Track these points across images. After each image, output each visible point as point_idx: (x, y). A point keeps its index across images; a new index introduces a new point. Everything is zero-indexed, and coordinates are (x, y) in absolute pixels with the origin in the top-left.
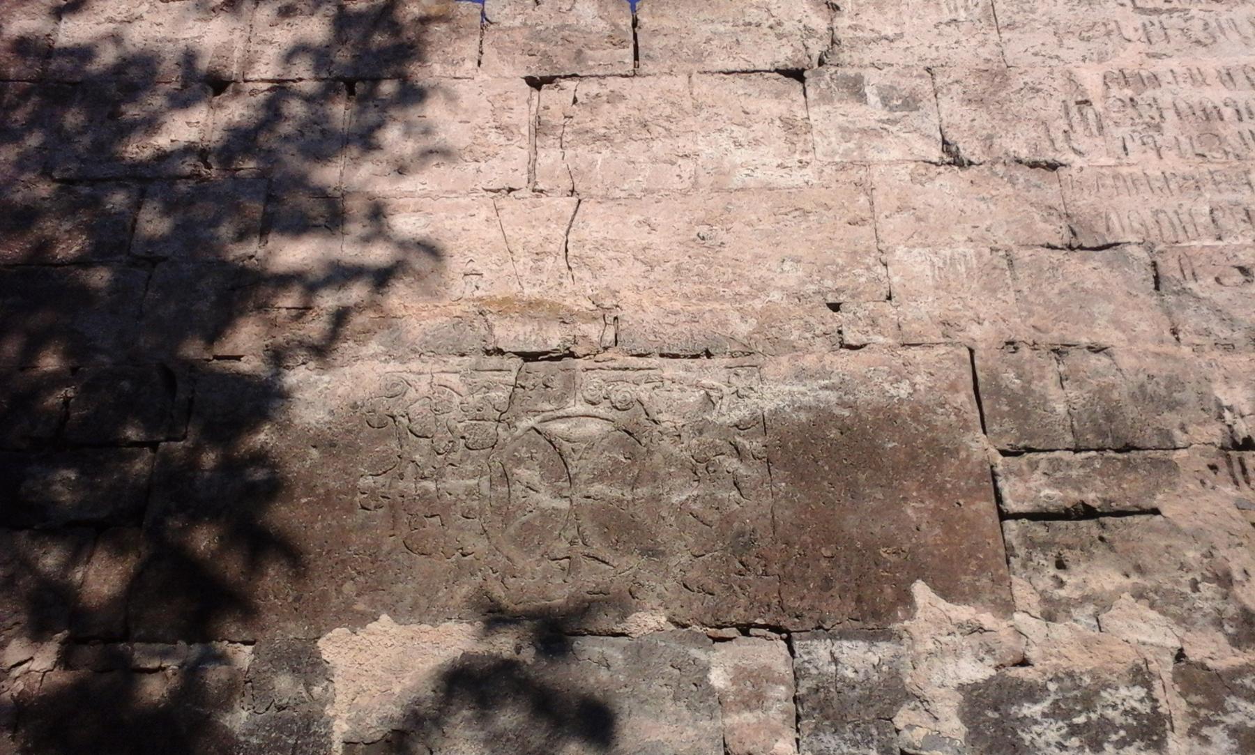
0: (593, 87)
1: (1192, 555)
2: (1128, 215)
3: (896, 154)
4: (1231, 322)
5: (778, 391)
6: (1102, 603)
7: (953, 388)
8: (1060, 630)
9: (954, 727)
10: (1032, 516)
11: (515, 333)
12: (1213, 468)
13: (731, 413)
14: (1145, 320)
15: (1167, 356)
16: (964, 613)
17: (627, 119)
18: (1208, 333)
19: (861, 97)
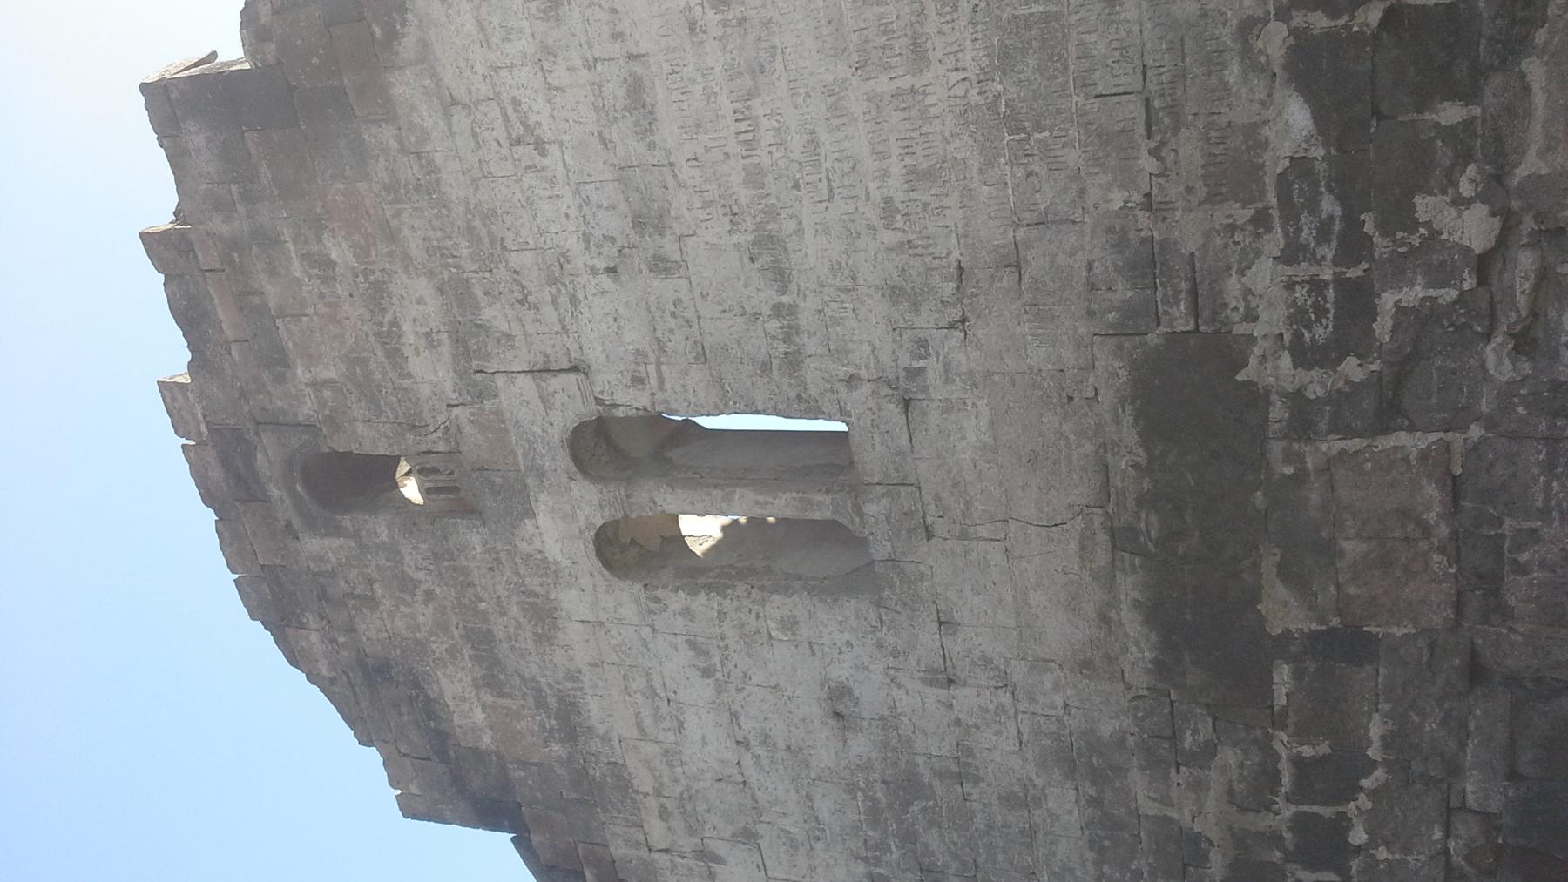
1: (1218, 241)
3: (962, 357)
5: (1130, 436)
6: (1247, 292)
7: (1120, 347)
8: (1264, 316)
9: (1315, 373)
10: (1197, 317)
11: (1102, 557)
12: (1164, 219)
13: (1142, 457)
15: (1093, 232)
16: (1253, 361)
17: (953, 494)
18: (1073, 201)
19: (921, 370)
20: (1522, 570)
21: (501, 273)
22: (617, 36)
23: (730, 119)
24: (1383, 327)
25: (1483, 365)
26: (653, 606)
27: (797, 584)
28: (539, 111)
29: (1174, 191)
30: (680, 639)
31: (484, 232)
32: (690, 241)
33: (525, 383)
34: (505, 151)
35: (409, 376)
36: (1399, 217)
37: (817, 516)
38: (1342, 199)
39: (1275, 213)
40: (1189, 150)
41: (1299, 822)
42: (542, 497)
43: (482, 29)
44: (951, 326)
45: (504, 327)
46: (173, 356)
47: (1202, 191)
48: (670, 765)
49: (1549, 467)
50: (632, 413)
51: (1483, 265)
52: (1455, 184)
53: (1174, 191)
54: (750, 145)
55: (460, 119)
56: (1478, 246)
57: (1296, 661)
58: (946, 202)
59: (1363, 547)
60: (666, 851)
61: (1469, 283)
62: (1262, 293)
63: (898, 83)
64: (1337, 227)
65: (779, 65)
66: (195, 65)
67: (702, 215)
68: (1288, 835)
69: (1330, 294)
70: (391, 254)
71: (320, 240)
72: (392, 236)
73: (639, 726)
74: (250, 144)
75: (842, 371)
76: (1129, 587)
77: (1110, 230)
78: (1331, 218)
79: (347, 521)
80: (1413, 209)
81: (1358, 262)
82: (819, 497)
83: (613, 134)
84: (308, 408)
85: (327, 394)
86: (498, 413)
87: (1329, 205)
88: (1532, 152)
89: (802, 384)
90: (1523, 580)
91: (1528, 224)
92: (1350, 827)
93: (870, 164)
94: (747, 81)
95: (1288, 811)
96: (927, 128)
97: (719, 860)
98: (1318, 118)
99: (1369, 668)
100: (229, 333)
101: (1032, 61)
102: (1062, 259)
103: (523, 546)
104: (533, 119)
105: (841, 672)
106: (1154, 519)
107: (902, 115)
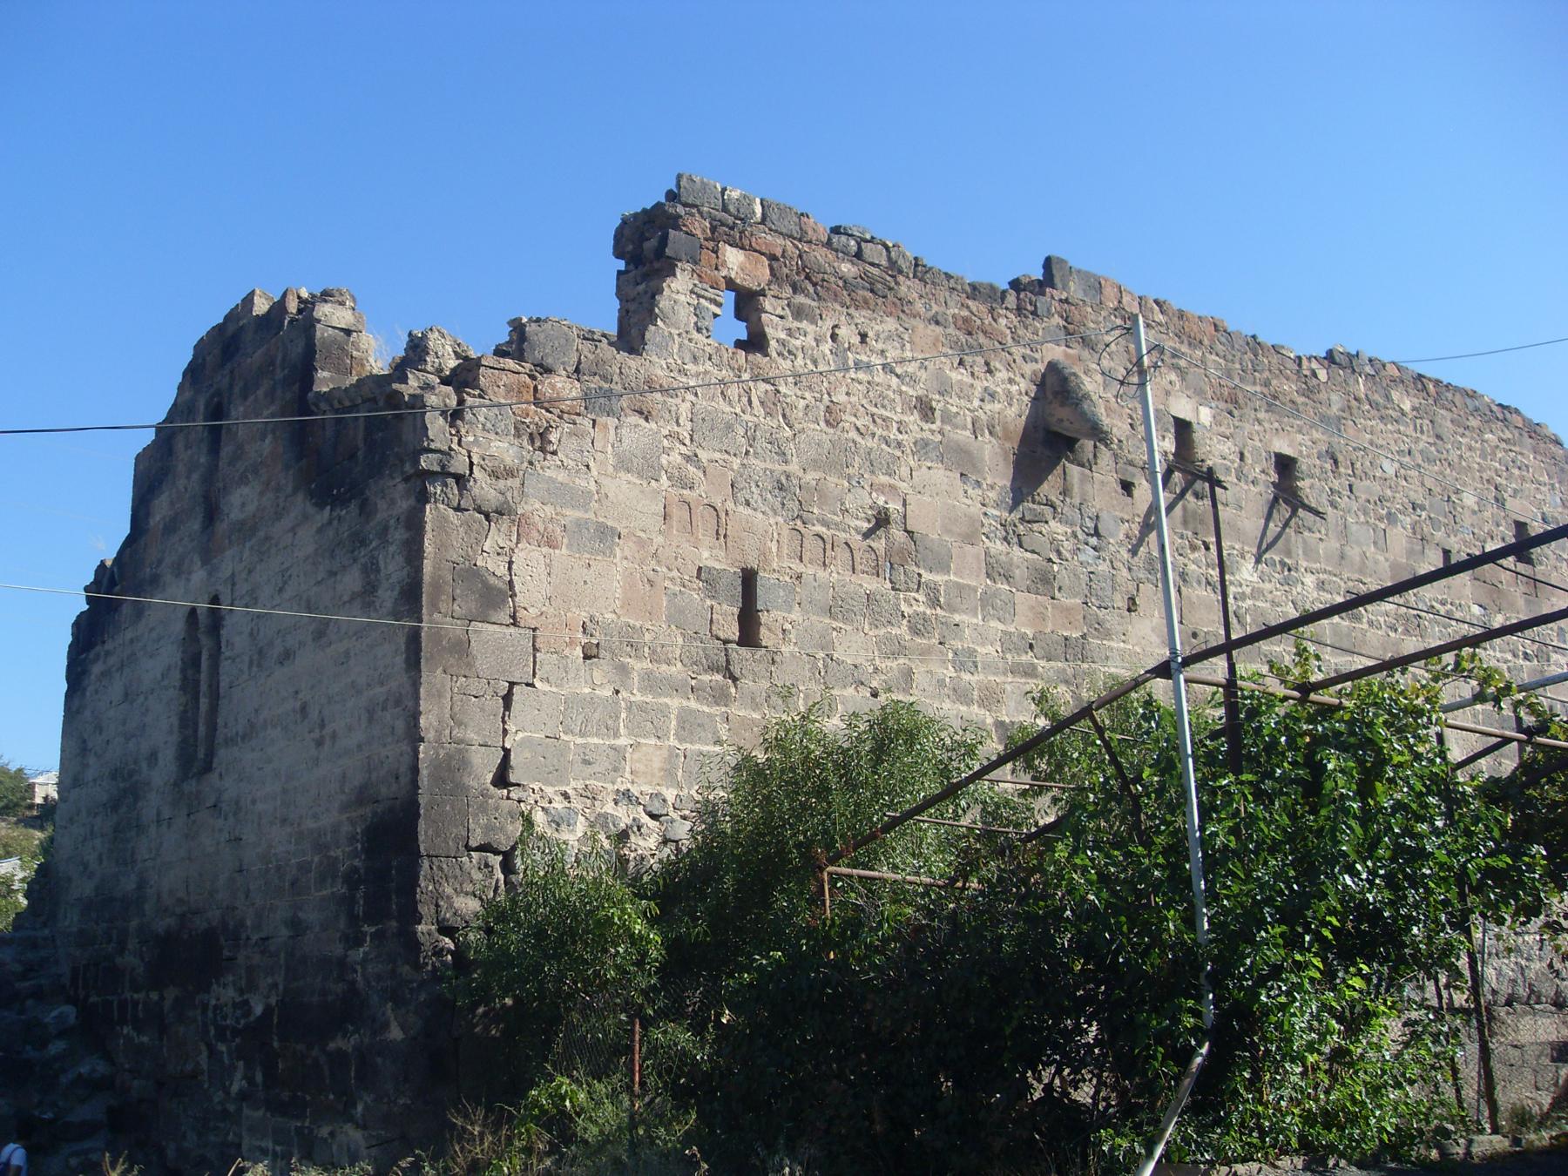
33: (228, 573)
40: (257, 959)
66: (342, 329)
105: (161, 762)
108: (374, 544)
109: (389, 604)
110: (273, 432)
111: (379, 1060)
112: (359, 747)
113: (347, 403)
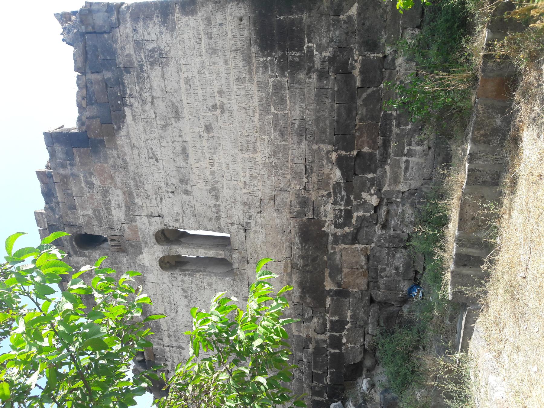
0: (249, 256)
2: (269, 192)
3: (260, 220)
4: (286, 184)
5: (297, 241)
6: (325, 211)
9: (339, 230)
11: (289, 270)
13: (300, 246)
14: (287, 196)
16: (326, 226)
19: (250, 223)
20: (382, 277)
21: (142, 190)
22: (180, 136)
23: (208, 159)
24: (354, 220)
25: (375, 230)
26: (173, 279)
27: (213, 274)
28: (158, 151)
29: (311, 187)
30: (180, 288)
31: (138, 180)
32: (194, 187)
33: (145, 219)
34: (147, 160)
35: (112, 215)
36: (358, 197)
37: (220, 257)
38: (346, 191)
39: (332, 193)
40: (314, 178)
41: (331, 337)
42: (146, 249)
43: (145, 130)
44: (258, 213)
45: (141, 204)
46: (40, 204)
47: (316, 187)
48: (172, 322)
49: (388, 254)
50: (174, 228)
51: (376, 209)
52: (370, 191)
53: (311, 187)
54: (212, 166)
55: (136, 151)
56: (375, 204)
57: (331, 296)
58: (259, 184)
59: (348, 270)
60: (168, 346)
61: (372, 212)
62: (329, 211)
63: (249, 155)
64: (345, 198)
65: (221, 147)
67: (198, 181)
68: (328, 340)
69: (343, 213)
70: (111, 183)
71: (91, 177)
72: (112, 178)
73: (165, 311)
74: (74, 151)
75: (230, 222)
76: (295, 278)
77: (296, 194)
78: (344, 196)
79: (87, 253)
80: (361, 195)
81: (349, 206)
82: (221, 252)
83: (177, 159)
84: (81, 221)
85: (87, 218)
86: (136, 226)
87: (344, 193)
88: (386, 185)
89: (220, 224)
90: (382, 279)
91: (385, 200)
92: (342, 338)
93: (241, 173)
94: (213, 151)
95: (328, 334)
96: (255, 167)
97: (183, 348)
98: (343, 174)
99: (348, 299)
100: (60, 200)
101: (281, 154)
102: (285, 200)
103: (138, 262)
104: (156, 153)
106: (302, 261)
107: (250, 163)
108: (143, 56)
109: (167, 37)
110: (91, 174)
111: (367, 23)
112: (226, 62)
113: (84, 92)
